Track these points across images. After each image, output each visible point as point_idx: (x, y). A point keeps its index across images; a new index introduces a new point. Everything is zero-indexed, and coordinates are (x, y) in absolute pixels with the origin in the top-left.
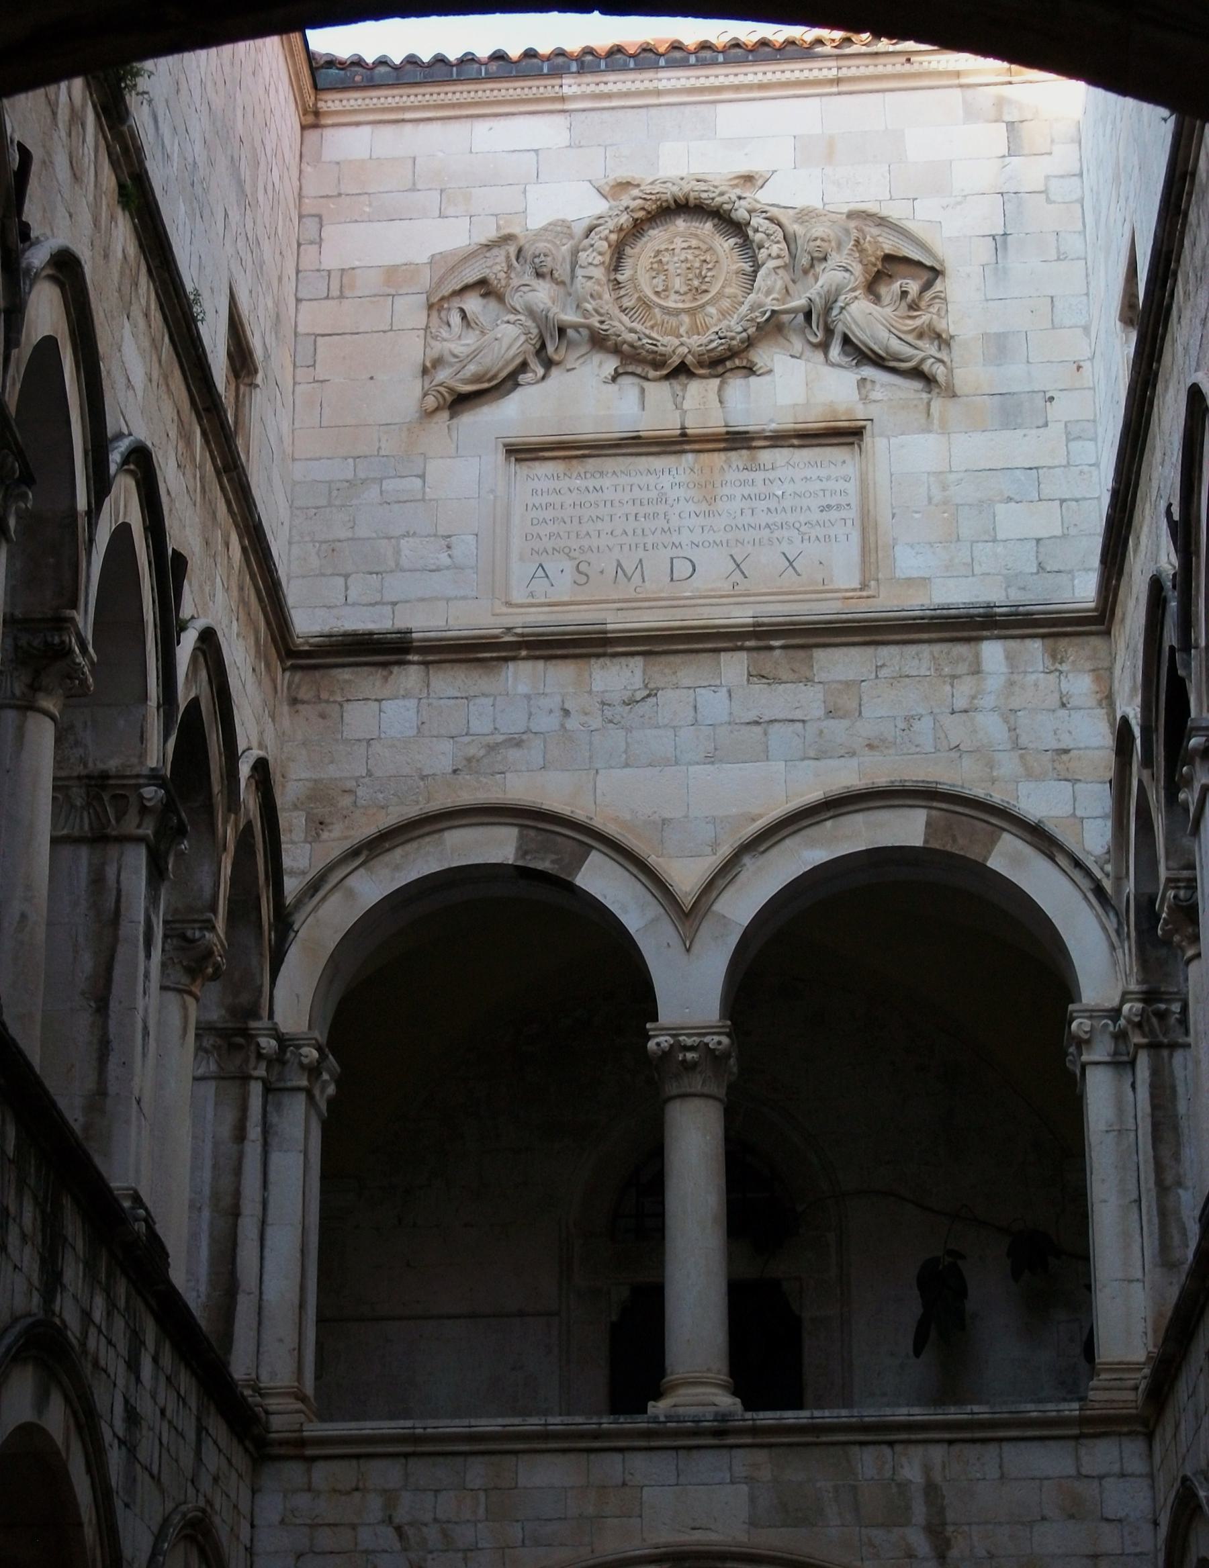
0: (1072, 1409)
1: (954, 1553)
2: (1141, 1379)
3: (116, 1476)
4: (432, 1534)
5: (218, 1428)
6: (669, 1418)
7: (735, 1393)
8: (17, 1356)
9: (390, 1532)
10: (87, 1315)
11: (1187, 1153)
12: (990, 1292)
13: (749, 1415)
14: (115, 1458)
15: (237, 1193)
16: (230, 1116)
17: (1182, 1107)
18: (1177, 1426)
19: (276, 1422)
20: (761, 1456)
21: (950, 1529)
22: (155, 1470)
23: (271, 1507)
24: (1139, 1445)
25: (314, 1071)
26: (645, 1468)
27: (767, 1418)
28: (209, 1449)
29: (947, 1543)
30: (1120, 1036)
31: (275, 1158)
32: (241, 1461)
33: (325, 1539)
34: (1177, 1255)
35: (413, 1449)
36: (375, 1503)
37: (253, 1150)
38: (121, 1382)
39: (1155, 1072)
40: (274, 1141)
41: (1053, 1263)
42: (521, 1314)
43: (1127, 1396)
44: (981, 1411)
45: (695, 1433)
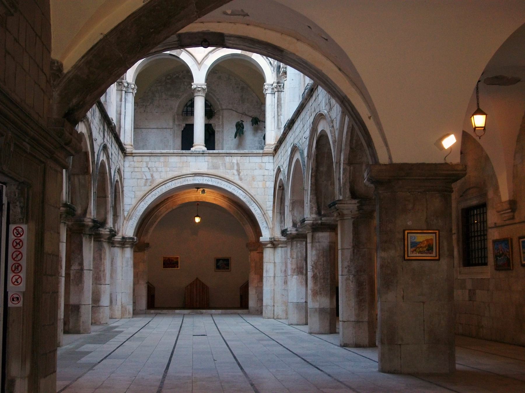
0: (261, 151)
1: (241, 174)
2: (273, 147)
4: (154, 169)
9: (147, 169)
11: (283, 110)
12: (248, 127)
15: (121, 111)
16: (119, 97)
17: (282, 102)
19: (128, 150)
23: (127, 164)
24: (272, 157)
25: (133, 89)
26: (190, 159)
29: (240, 173)
30: (273, 89)
31: (127, 104)
32: (123, 157)
33: (136, 170)
34: (280, 127)
35: (151, 155)
36: (145, 164)
37: (123, 103)
39: (278, 96)
40: (127, 101)
41: (258, 122)
42: (166, 128)
43: (271, 150)
44: (246, 151)
45: (199, 154)
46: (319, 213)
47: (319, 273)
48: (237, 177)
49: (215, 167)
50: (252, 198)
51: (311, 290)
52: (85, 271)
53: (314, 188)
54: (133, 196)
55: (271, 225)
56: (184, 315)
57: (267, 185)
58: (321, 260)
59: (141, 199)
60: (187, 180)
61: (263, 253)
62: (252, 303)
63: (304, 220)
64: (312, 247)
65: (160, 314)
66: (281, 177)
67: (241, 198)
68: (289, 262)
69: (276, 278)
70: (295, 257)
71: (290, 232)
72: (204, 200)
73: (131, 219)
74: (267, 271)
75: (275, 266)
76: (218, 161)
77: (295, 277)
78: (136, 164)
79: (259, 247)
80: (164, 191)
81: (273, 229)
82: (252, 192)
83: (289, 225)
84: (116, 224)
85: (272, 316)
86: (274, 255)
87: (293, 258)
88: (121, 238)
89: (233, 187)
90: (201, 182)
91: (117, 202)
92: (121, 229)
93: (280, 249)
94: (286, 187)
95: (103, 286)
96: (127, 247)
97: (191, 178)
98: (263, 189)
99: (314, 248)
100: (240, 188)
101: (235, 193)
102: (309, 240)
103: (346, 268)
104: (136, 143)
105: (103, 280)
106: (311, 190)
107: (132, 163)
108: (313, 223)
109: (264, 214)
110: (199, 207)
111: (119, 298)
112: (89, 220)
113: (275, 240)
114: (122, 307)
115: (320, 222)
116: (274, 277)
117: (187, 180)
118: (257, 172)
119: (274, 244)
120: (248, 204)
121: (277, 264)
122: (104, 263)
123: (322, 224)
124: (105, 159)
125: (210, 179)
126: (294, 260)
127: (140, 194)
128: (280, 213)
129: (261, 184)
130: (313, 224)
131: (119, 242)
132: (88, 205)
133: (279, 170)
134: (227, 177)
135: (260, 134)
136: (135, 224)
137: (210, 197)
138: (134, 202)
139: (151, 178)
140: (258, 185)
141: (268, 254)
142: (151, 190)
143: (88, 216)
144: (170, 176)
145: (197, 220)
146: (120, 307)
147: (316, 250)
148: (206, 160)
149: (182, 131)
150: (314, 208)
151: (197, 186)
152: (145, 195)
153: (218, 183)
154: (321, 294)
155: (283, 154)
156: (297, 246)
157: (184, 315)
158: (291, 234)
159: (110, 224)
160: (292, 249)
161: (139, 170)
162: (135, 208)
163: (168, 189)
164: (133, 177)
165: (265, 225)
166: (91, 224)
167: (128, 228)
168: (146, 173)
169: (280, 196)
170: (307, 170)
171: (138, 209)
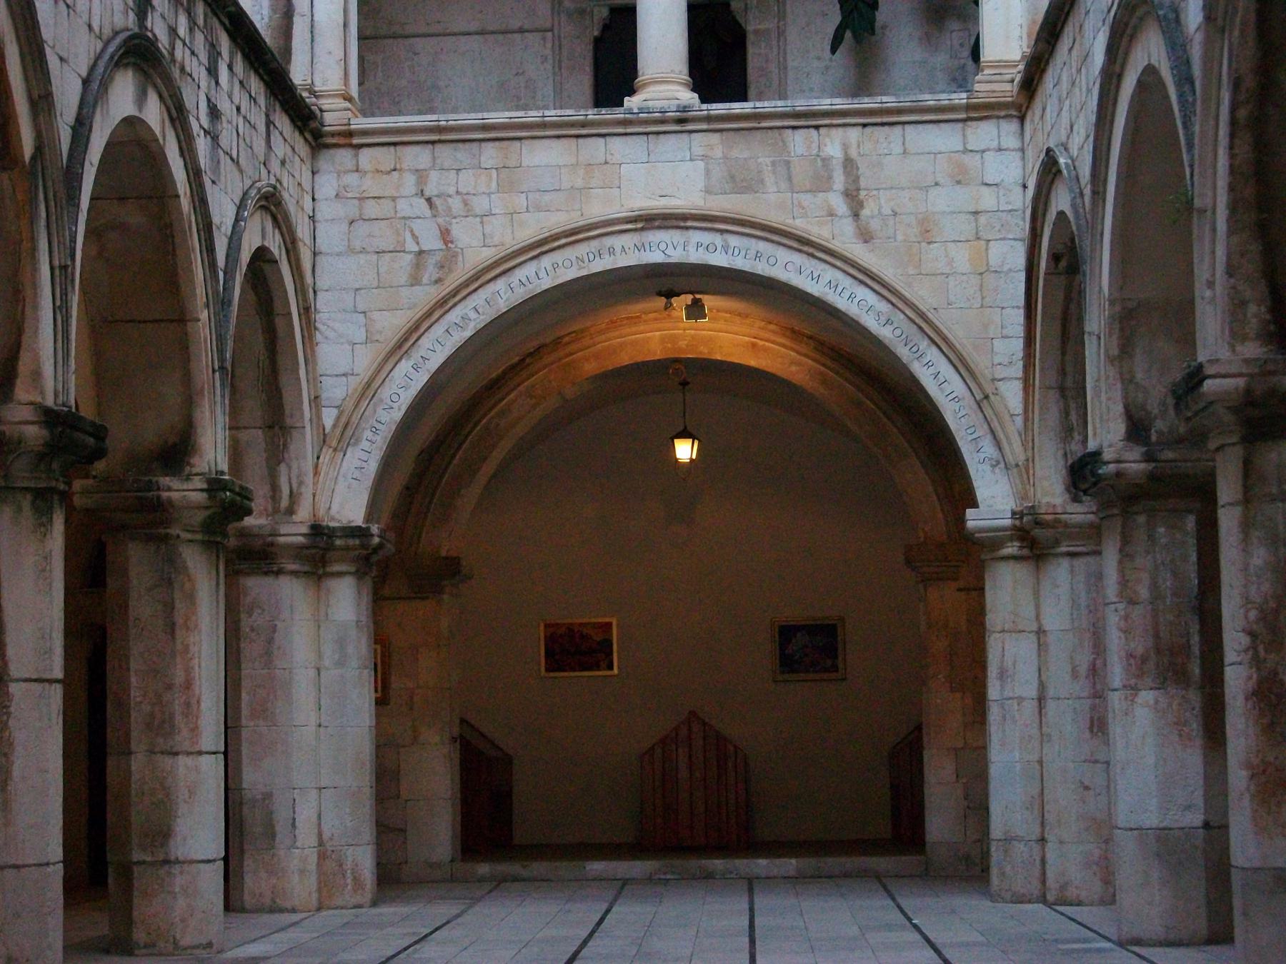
0: (960, 98)
1: (865, 212)
2: (1017, 74)
3: (203, 161)
4: (456, 204)
5: (283, 122)
6: (641, 111)
7: (693, 90)
8: (119, 62)
10: (173, 31)
13: (705, 106)
14: (202, 145)
18: (1044, 109)
19: (329, 118)
20: (715, 138)
21: (863, 193)
22: (235, 156)
23: (327, 185)
24: (1013, 126)
27: (719, 108)
28: (275, 137)
29: (861, 205)
32: (302, 149)
33: (372, 209)
35: (438, 137)
36: (410, 181)
38: (203, 84)
42: (521, 31)
44: (889, 101)
45: (663, 122)
48: (847, 227)
49: (743, 183)
50: (924, 324)
51: (1248, 765)
52: (14, 688)
54: (360, 335)
55: (1016, 451)
56: (626, 882)
57: (994, 259)
59: (399, 346)
60: (611, 251)
61: (983, 589)
62: (940, 824)
63: (1195, 377)
64: (1246, 526)
65: (516, 879)
66: (1061, 201)
67: (870, 323)
68: (1113, 619)
69: (1051, 706)
70: (1144, 593)
71: (1112, 468)
72: (704, 352)
73: (355, 440)
74: (1002, 675)
75: (1042, 647)
76: (754, 152)
77: (1147, 696)
78: (371, 185)
79: (959, 559)
80: (503, 305)
81: (1024, 472)
82: (923, 295)
83: (1106, 432)
84: (283, 468)
85: (1035, 887)
86: (1037, 594)
87: (1132, 602)
88: (305, 530)
89: (830, 274)
90: (676, 256)
91: (282, 360)
92: (307, 492)
93: (1065, 563)
94: (1085, 245)
95: (182, 760)
96: (340, 574)
97: (627, 240)
98: (975, 280)
99: (1256, 534)
100: (867, 277)
101: (841, 303)
102: (1228, 490)
104: (372, 95)
105: (185, 733)
106: (1233, 208)
107: (352, 179)
108: (1248, 391)
109: (983, 400)
110: (690, 385)
111: (306, 815)
112: (25, 413)
113: (1038, 523)
114: (322, 856)
116: (1041, 700)
117: (611, 251)
118: (941, 200)
119: (1034, 539)
120: (903, 352)
121: (1051, 638)
122: (186, 649)
124: (153, 114)
125: (717, 239)
126: (1138, 612)
127: (392, 324)
128: (1062, 390)
129: (962, 258)
131: (298, 552)
132: (20, 332)
133: (1050, 170)
134: (800, 225)
135: (954, 35)
136: (373, 466)
137: (727, 334)
138: (364, 361)
139: (439, 245)
140: (951, 262)
141: (1007, 590)
142: (443, 304)
143: (22, 392)
144: (530, 230)
145: (685, 450)
146: (313, 859)
148: (698, 151)
149: (598, 42)
150: (1252, 309)
151: (667, 282)
152: (416, 327)
153: (758, 256)
155: (1065, 85)
156: (1151, 538)
157: (626, 882)
158: (1118, 474)
159: (212, 451)
160: (1125, 556)
161: (385, 208)
162: (369, 390)
163: (521, 294)
164: (357, 245)
165: (989, 449)
166: (34, 433)
167: (341, 486)
168: (417, 226)
169: (1057, 311)
170: (1205, 101)
171: (385, 393)
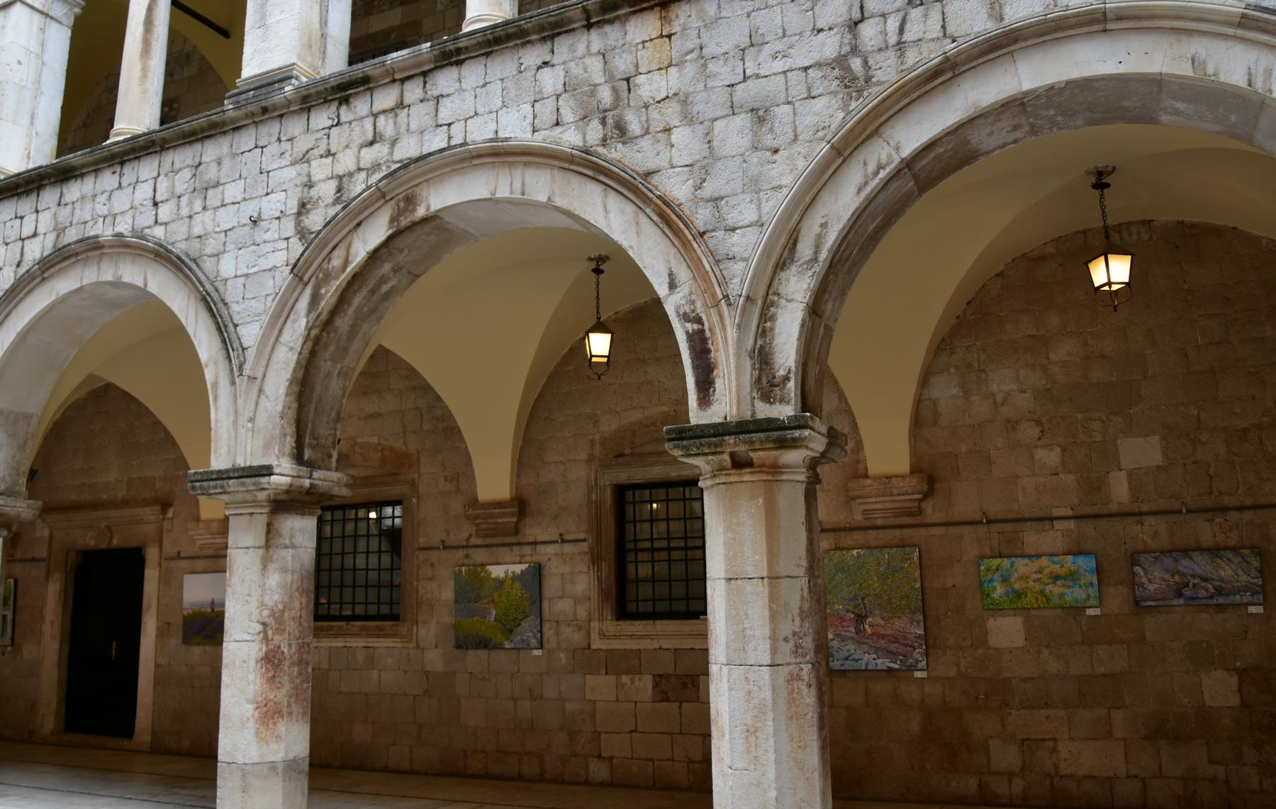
46: (298, 458)
47: (290, 646)
53: (300, 375)
58: (297, 604)
99: (271, 567)
103: (786, 640)
108: (291, 485)
115: (307, 482)
123: (311, 491)
130: (290, 490)
147: (283, 570)
150: (288, 438)
154: (290, 713)
